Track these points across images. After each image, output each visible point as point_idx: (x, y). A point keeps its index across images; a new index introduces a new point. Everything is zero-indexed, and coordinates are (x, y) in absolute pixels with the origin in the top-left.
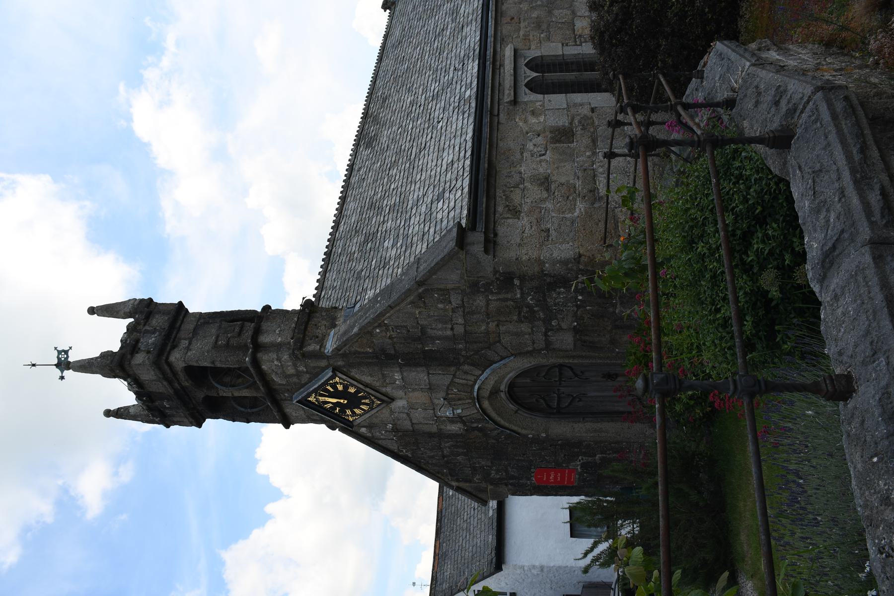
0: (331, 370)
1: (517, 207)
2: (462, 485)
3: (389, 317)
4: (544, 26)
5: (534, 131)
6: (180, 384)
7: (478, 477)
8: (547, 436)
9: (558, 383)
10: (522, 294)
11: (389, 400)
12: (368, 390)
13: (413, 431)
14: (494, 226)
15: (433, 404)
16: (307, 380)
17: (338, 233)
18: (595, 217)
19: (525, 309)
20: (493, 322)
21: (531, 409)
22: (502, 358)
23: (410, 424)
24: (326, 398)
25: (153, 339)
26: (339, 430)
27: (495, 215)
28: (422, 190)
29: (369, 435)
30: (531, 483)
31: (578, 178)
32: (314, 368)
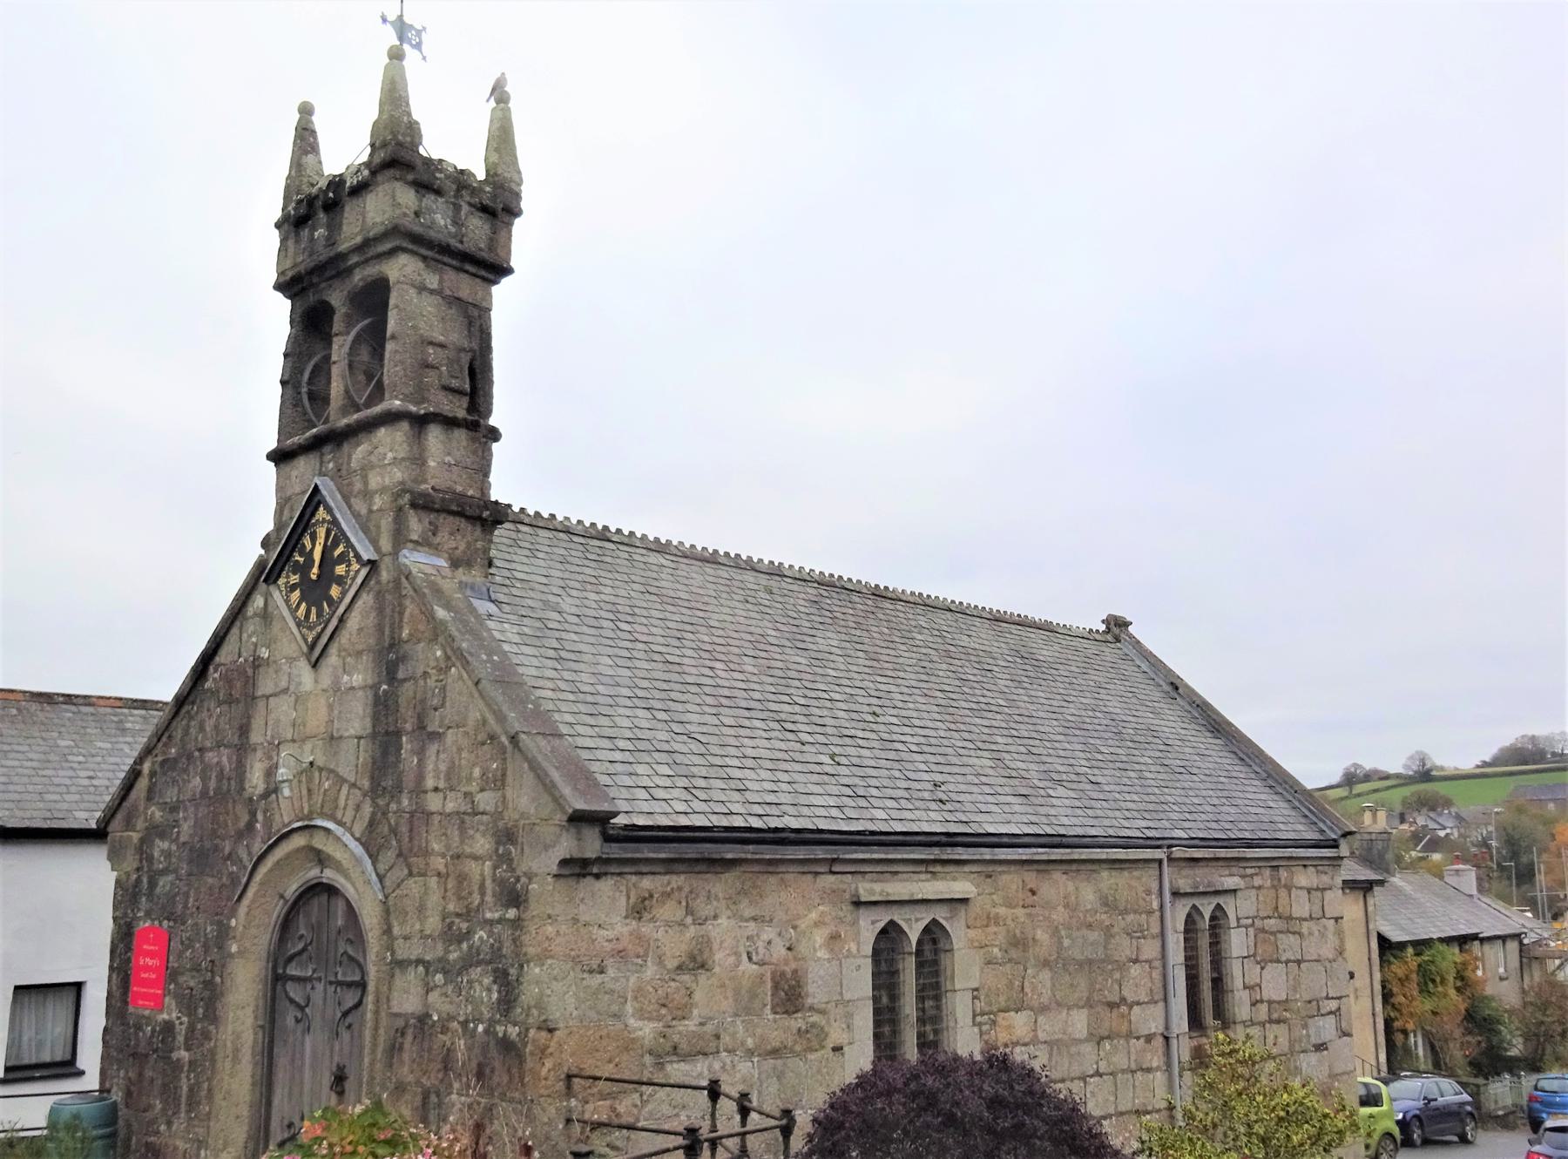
0: (372, 558)
1: (650, 913)
2: (142, 784)
3: (461, 677)
4: (1014, 954)
5: (798, 940)
6: (357, 265)
7: (158, 814)
8: (231, 956)
9: (333, 979)
10: (491, 923)
11: (313, 659)
12: (334, 622)
13: (254, 698)
14: (613, 874)
15: (303, 741)
16: (357, 508)
17: (644, 552)
18: (625, 1057)
19: (464, 926)
20: (446, 866)
21: (286, 925)
22: (381, 878)
23: (268, 693)
24: (322, 541)
25: (442, 223)
26: (261, 556)
27: (635, 873)
28: (701, 729)
29: (250, 611)
30: (140, 919)
31: (702, 1024)
32: (378, 527)
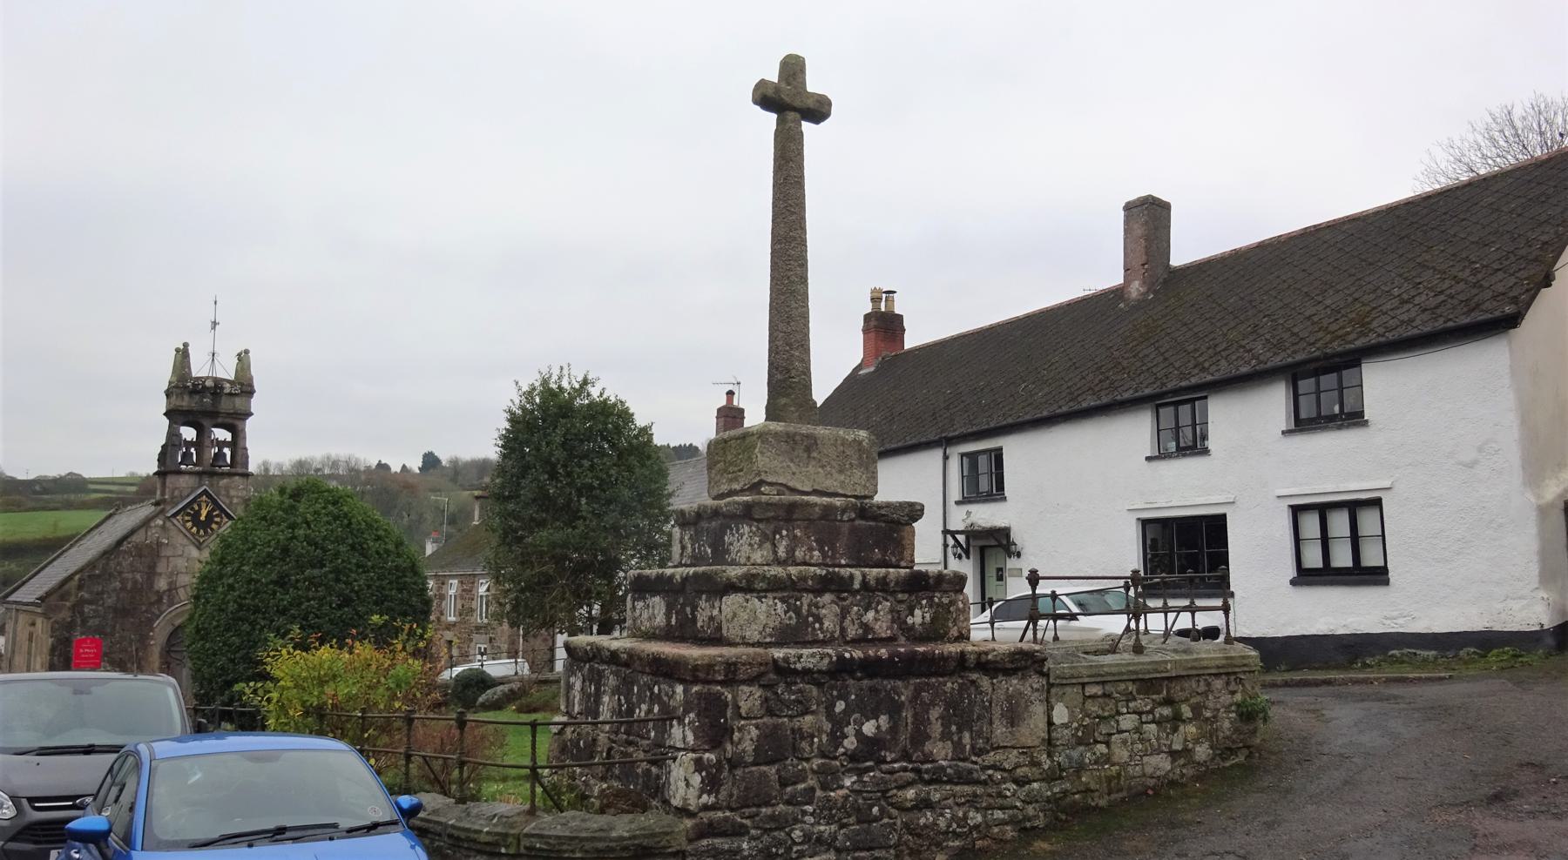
29: (153, 524)
